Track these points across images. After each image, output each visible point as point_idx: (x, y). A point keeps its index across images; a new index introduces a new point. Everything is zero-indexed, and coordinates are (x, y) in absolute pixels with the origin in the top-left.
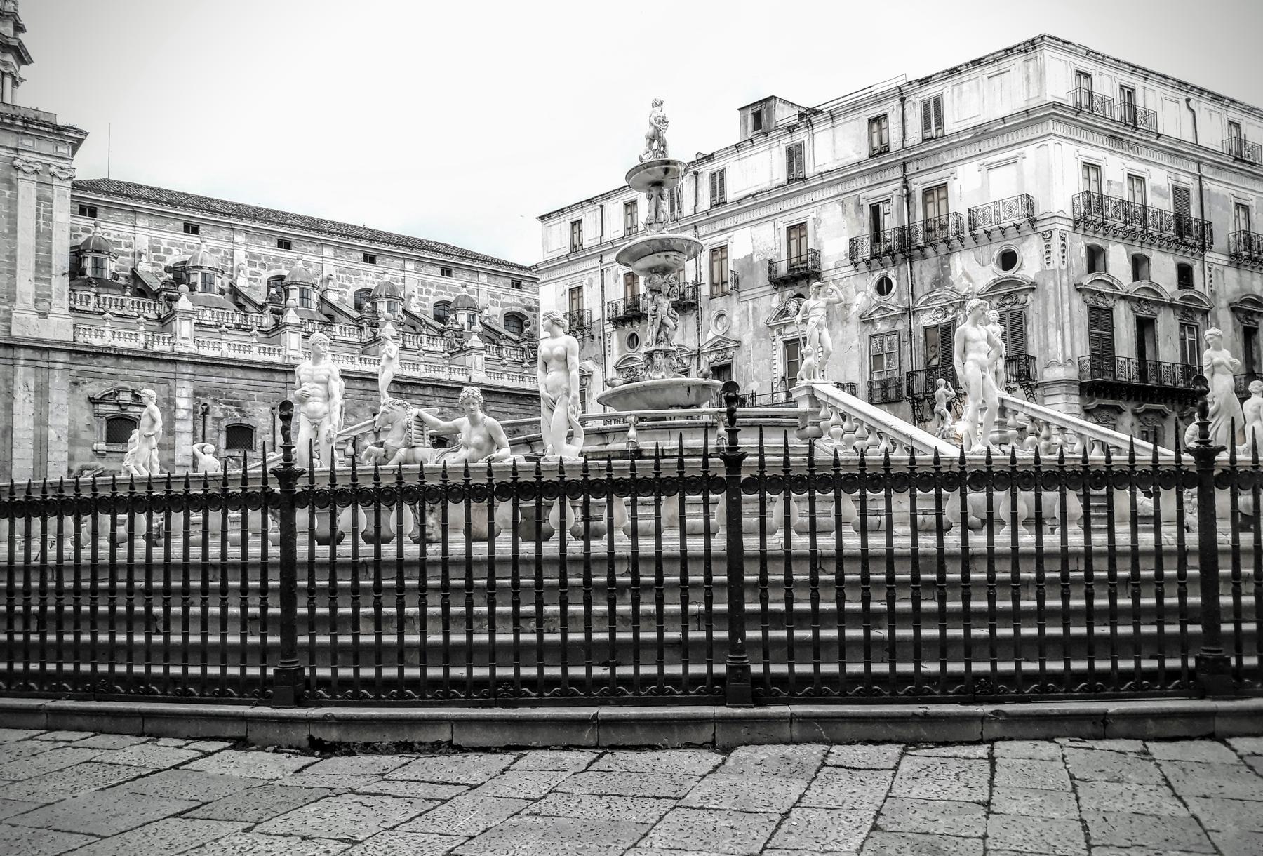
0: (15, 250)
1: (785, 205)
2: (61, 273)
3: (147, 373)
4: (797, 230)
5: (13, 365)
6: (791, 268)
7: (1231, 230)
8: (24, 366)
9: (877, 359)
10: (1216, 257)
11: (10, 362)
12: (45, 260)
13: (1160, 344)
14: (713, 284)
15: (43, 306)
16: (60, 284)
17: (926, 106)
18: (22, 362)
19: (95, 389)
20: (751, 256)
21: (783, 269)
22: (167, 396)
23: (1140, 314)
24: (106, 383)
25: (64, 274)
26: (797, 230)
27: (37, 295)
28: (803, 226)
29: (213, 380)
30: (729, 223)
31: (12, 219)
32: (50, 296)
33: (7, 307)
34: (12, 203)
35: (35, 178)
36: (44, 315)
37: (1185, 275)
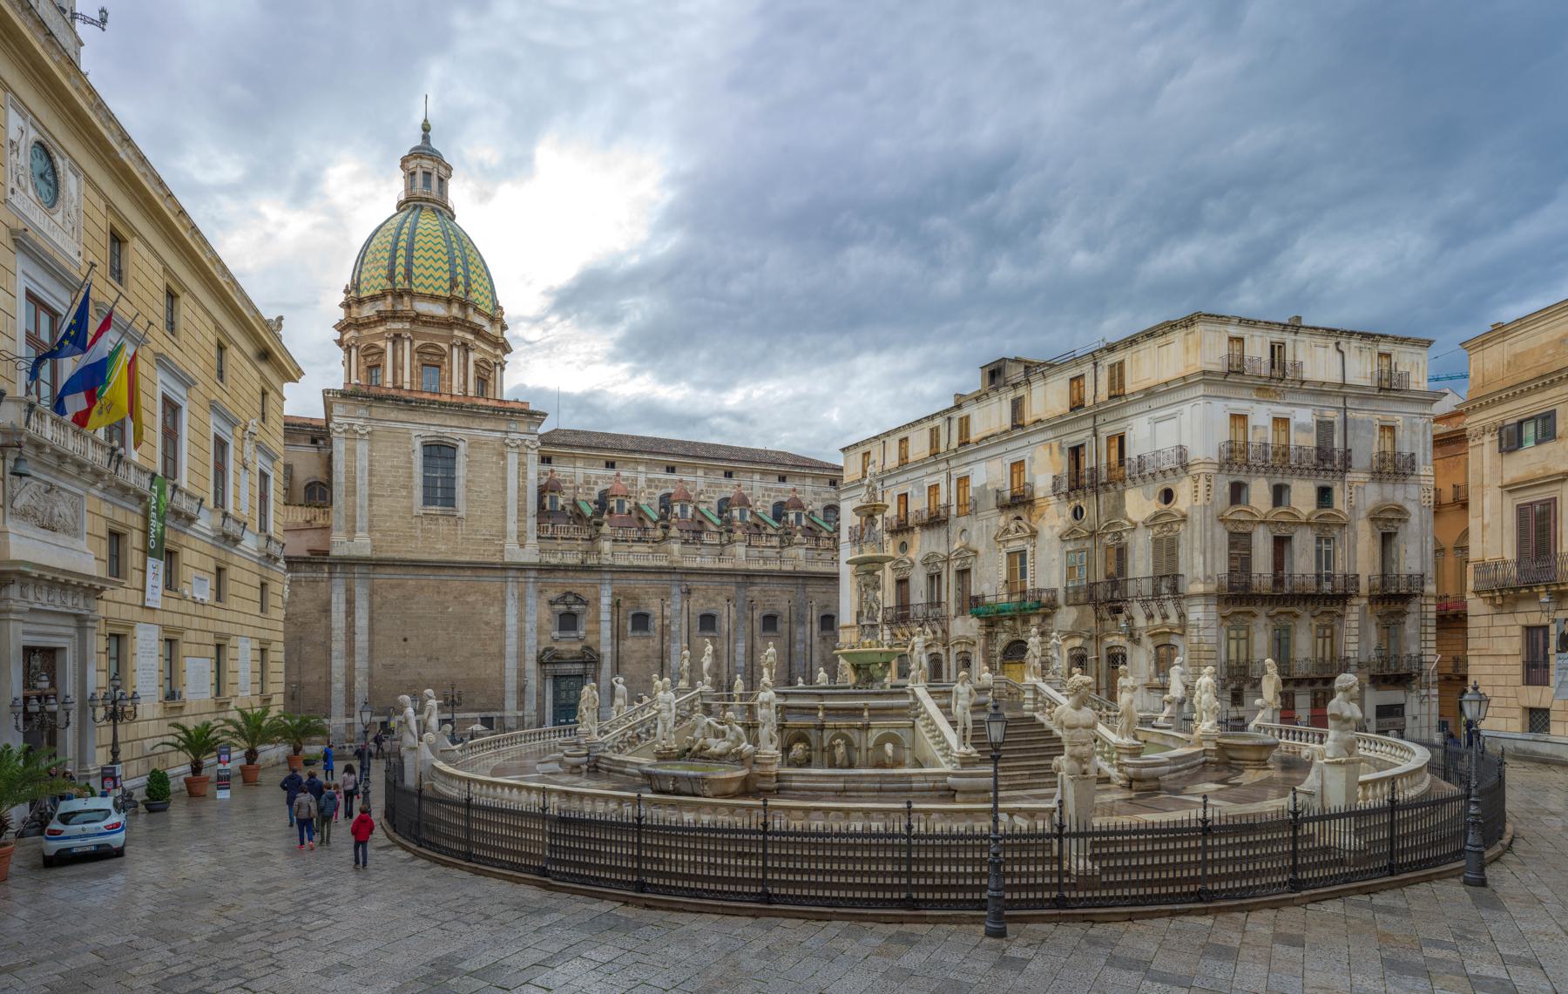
1: (1011, 446)
4: (1018, 466)
6: (1013, 497)
7: (1375, 450)
9: (1071, 569)
10: (1357, 476)
13: (1296, 557)
14: (958, 505)
16: (532, 523)
17: (1112, 366)
19: (553, 594)
20: (985, 485)
21: (1008, 495)
23: (1278, 534)
24: (559, 589)
26: (1018, 466)
28: (1022, 463)
29: (625, 583)
30: (971, 458)
37: (1324, 495)
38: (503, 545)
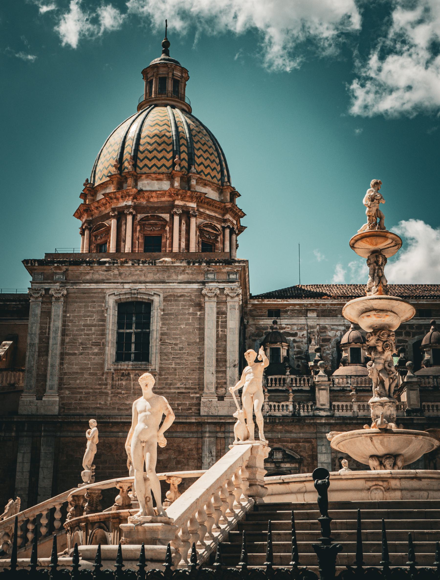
0: (203, 353)
2: (232, 365)
3: (294, 435)
5: (202, 437)
8: (209, 437)
11: (199, 435)
12: (222, 357)
15: (221, 391)
18: (207, 435)
22: (310, 453)
25: (234, 366)
27: (217, 383)
31: (202, 330)
32: (225, 383)
33: (198, 395)
34: (202, 320)
35: (215, 299)
36: (221, 398)
38: (199, 399)
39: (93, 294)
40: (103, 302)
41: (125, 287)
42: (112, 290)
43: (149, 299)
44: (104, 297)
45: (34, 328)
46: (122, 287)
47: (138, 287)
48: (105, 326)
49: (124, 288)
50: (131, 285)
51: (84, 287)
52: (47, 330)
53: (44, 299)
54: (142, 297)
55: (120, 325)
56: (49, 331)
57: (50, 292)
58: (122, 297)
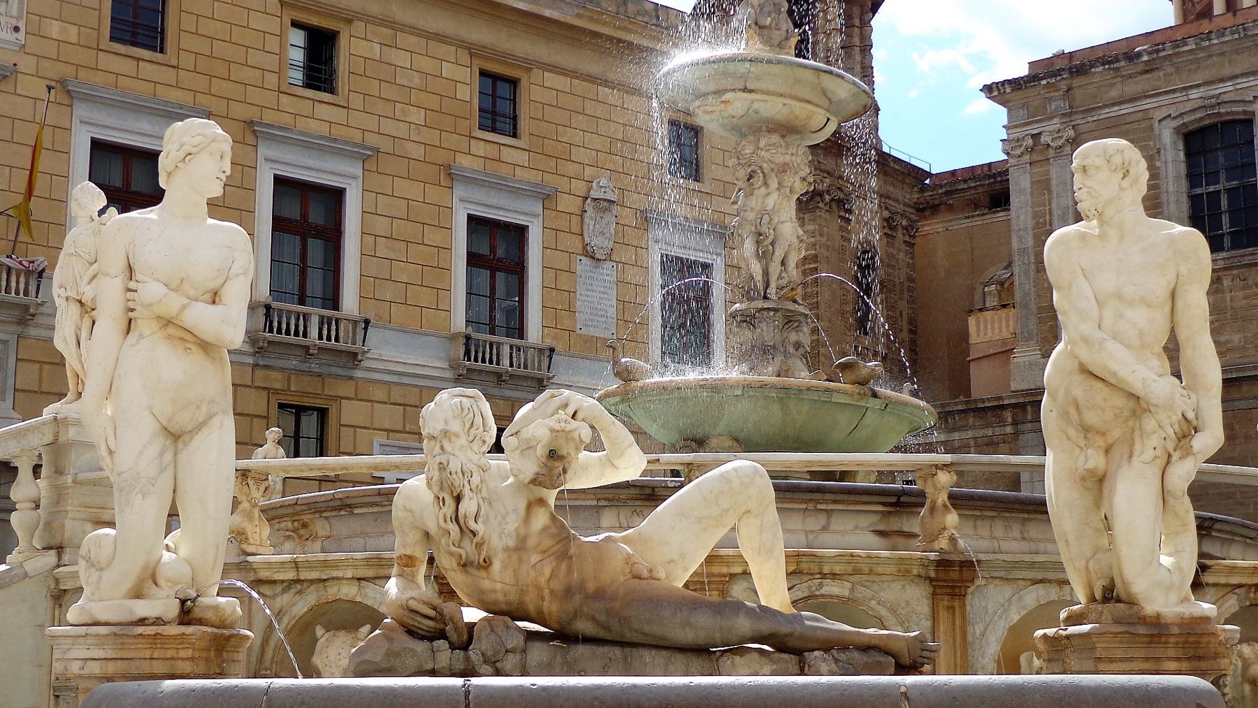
39: (1127, 126)
40: (1150, 139)
41: (1191, 97)
42: (1164, 109)
43: (1245, 112)
44: (1151, 128)
45: (1022, 218)
46: (1185, 98)
47: (1217, 92)
48: (1159, 189)
49: (1189, 100)
50: (1202, 89)
51: (1109, 115)
52: (1048, 217)
53: (1035, 157)
54: (1229, 110)
55: (1193, 178)
56: (1051, 219)
57: (1045, 139)
58: (1186, 119)
